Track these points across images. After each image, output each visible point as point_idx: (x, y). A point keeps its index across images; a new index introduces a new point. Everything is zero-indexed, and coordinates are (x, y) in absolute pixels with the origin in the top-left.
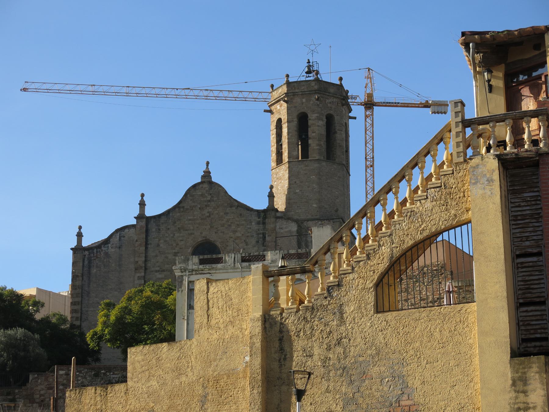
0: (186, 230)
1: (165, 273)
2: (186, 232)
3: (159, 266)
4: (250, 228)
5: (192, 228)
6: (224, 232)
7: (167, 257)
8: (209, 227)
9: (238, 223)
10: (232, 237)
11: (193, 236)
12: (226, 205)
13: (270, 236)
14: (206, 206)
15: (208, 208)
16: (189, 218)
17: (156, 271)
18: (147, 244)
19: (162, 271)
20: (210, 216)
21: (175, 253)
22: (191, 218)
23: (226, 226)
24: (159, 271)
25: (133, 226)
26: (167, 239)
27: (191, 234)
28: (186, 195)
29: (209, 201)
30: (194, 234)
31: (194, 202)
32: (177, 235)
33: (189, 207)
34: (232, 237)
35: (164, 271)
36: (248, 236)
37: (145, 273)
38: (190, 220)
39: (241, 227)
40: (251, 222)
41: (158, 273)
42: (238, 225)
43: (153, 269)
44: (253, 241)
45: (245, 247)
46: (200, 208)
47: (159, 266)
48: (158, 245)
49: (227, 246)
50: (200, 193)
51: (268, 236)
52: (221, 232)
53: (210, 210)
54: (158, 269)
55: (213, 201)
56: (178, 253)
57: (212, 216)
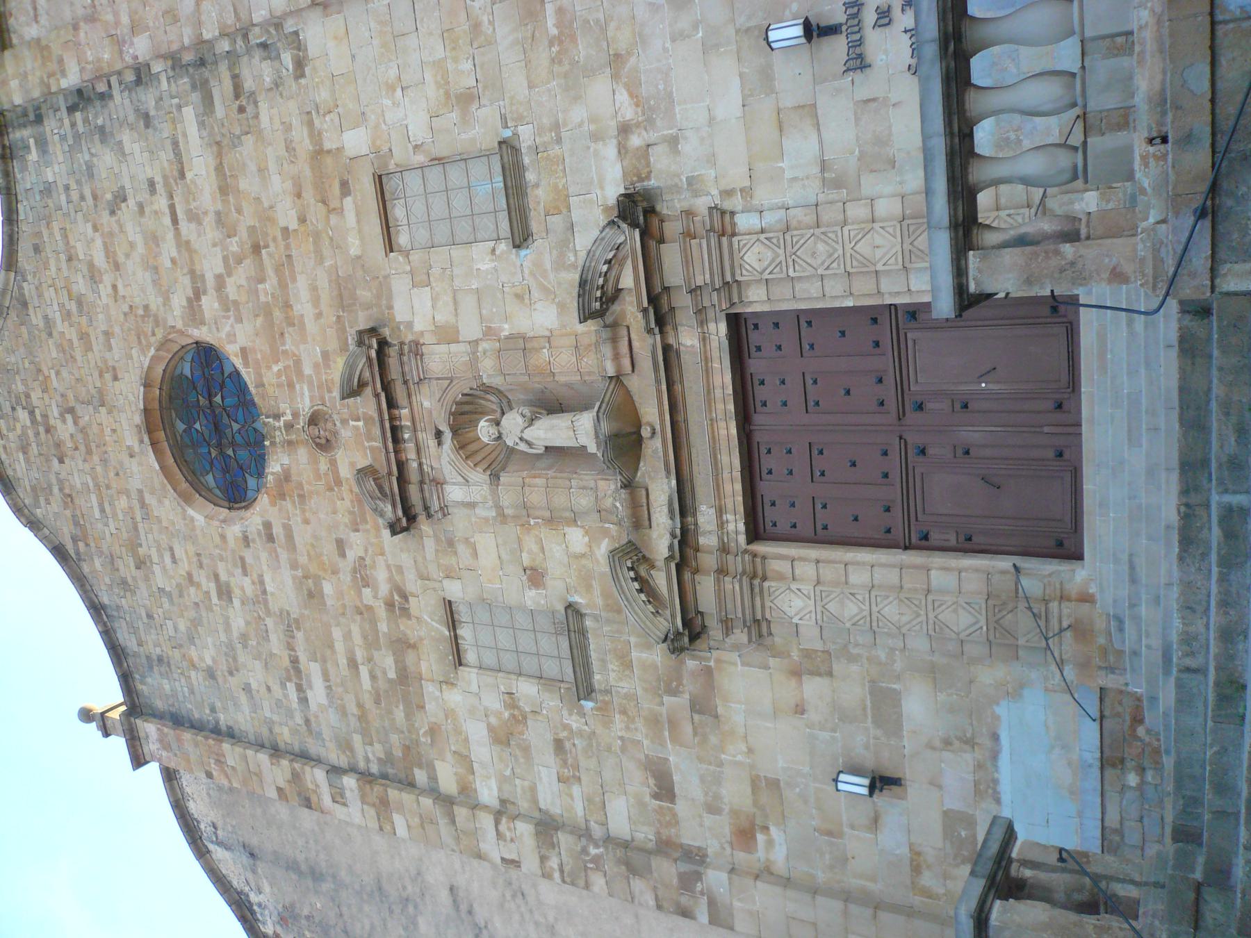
0: (136, 529)
1: (303, 658)
2: (140, 526)
3: (283, 686)
4: (67, 188)
5: (122, 503)
6: (107, 334)
7: (244, 638)
8: (103, 410)
9: (63, 257)
10: (114, 287)
11: (148, 499)
12: (24, 329)
13: (61, 61)
14: (48, 431)
15: (52, 422)
16: (97, 515)
17: (304, 700)
18: (217, 732)
19: (298, 671)
20: (71, 411)
21: (220, 595)
22: (94, 498)
23: (84, 320)
24: (300, 688)
25: (170, 776)
26: (182, 627)
27: (143, 505)
28: (34, 525)
29: (32, 413)
30: (140, 492)
31: (50, 487)
32: (160, 580)
33: (68, 513)
34: (114, 287)
35: (295, 661)
36: (95, 197)
37: (318, 761)
38: (103, 511)
39: (72, 243)
40: (47, 190)
41: (310, 694)
42: (70, 259)
43: (299, 720)
44: (106, 159)
45: (131, 202)
46: (61, 461)
47: (283, 686)
48: (211, 674)
49: (146, 307)
50: (21, 455)
51: (63, 73)
52: (110, 349)
53: (56, 413)
54: (291, 687)
55: (28, 396)
56: (216, 576)
57: (72, 404)
